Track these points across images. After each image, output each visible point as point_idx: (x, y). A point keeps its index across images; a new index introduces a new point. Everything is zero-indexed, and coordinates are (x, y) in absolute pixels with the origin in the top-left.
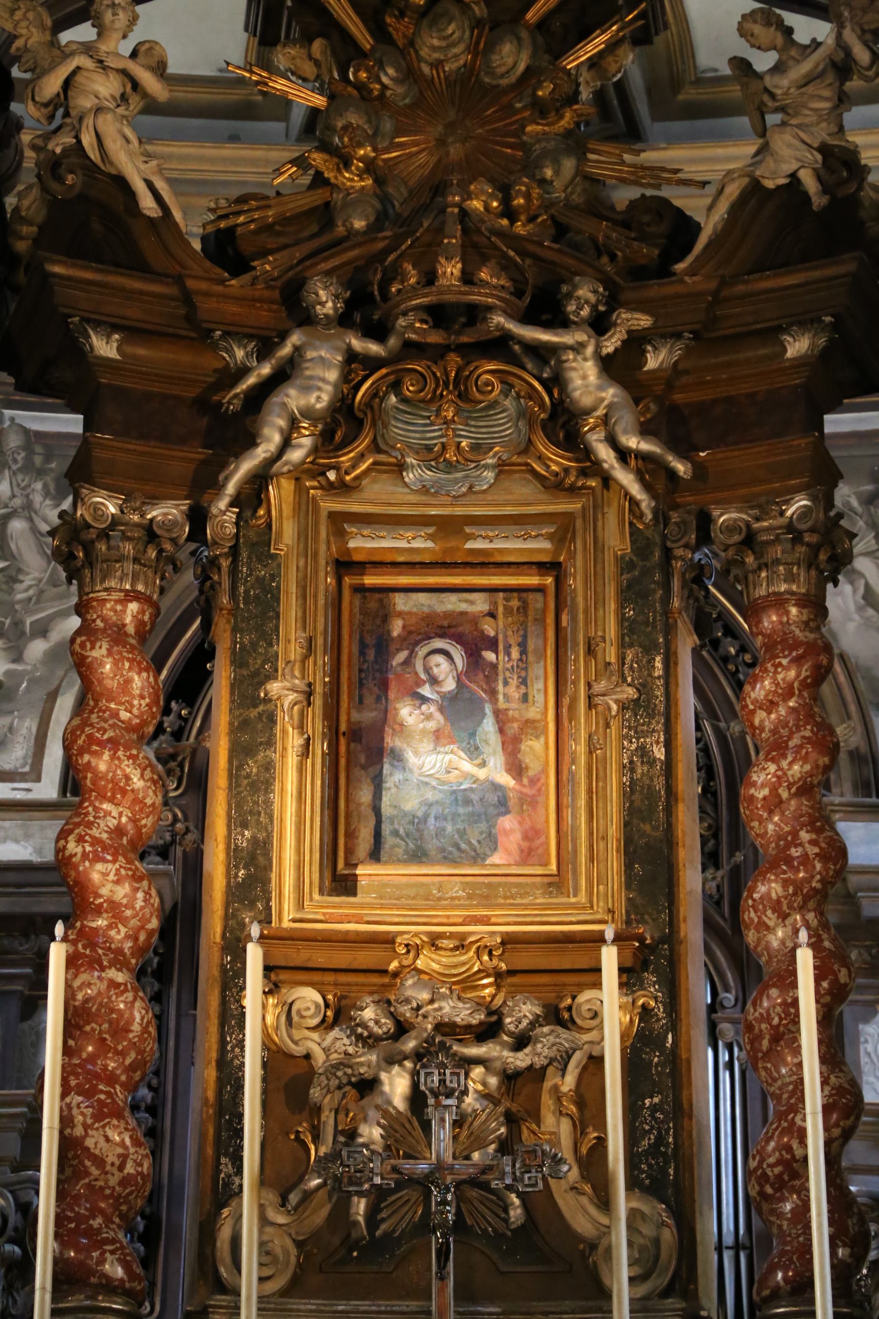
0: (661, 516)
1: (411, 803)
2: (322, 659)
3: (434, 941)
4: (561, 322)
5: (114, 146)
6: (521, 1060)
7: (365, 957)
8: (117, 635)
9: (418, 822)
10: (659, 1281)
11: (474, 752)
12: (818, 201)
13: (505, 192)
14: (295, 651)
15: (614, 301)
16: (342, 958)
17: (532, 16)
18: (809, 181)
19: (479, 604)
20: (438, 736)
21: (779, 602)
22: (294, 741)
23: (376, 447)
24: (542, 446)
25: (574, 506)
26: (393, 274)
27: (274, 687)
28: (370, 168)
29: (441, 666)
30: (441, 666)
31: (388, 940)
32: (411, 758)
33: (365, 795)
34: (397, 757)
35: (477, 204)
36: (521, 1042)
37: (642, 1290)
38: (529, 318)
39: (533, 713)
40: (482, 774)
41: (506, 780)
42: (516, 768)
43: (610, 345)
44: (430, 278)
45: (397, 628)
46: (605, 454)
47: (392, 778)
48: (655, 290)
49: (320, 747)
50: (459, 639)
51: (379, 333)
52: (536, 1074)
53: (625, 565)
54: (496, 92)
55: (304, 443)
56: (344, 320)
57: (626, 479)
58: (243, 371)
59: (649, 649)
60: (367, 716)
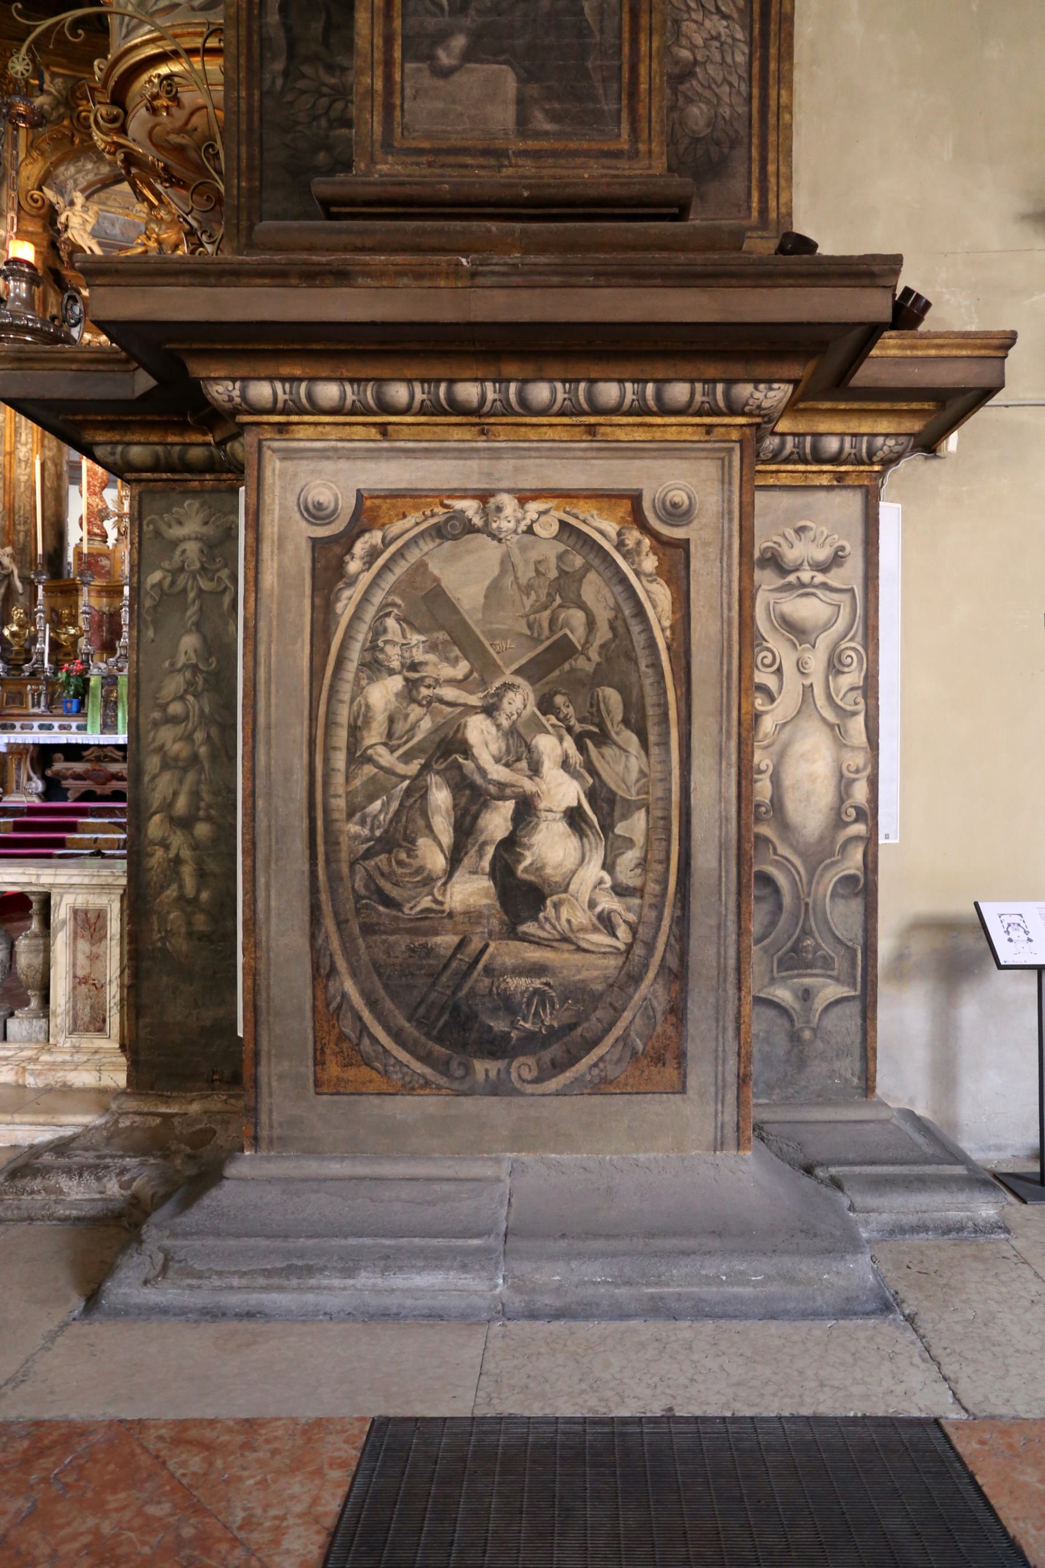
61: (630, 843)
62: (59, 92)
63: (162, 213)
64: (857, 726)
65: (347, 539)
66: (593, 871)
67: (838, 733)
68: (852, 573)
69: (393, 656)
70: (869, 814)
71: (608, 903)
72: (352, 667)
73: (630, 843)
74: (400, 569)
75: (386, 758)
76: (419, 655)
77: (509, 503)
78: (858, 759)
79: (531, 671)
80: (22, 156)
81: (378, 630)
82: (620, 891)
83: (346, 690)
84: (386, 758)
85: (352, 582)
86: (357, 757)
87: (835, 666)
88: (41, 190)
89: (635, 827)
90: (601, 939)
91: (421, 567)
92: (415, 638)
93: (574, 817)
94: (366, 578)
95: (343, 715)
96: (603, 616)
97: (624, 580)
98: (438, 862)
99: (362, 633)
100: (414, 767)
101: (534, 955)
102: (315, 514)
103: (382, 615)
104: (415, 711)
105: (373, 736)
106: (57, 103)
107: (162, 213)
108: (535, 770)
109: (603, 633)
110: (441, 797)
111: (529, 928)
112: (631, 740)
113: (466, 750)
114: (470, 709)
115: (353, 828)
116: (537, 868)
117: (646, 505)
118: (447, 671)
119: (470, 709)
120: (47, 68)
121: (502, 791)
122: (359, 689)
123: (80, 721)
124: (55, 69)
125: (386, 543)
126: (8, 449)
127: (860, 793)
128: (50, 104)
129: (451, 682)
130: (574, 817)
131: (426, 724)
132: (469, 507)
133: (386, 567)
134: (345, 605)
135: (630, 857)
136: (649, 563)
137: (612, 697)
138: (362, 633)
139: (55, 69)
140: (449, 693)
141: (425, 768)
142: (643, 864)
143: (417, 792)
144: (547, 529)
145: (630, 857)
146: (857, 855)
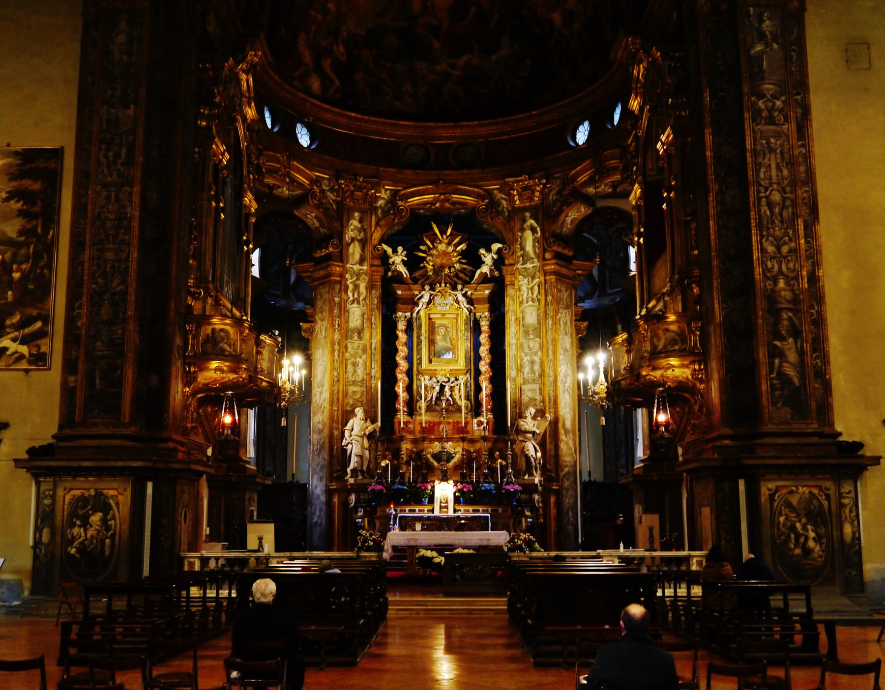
0: (470, 314)
1: (439, 349)
2: (427, 332)
3: (442, 370)
4: (458, 290)
5: (400, 269)
6: (452, 385)
7: (433, 372)
8: (402, 331)
9: (439, 352)
10: (469, 410)
11: (446, 342)
12: (489, 276)
13: (450, 270)
14: (424, 332)
15: (463, 287)
16: (431, 372)
17: (454, 243)
18: (488, 273)
19: (447, 322)
20: (442, 341)
21: (484, 326)
22: (424, 344)
23: (434, 304)
24: (455, 304)
25: (459, 312)
26: (436, 284)
27: (422, 337)
28: (432, 266)
29: (442, 330)
30: (442, 330)
31: (436, 370)
32: (439, 343)
33: (433, 348)
34: (437, 343)
35: (446, 272)
36: (452, 383)
37: (466, 412)
38: (453, 290)
39: (454, 337)
40: (447, 345)
41: (451, 346)
42: (452, 344)
43: (463, 292)
44: (441, 286)
45: (436, 325)
46: (463, 307)
47: (436, 346)
48: (469, 286)
49: (427, 344)
50: (444, 327)
51: (434, 291)
52: (454, 386)
53: (465, 320)
54: (449, 253)
55: (425, 306)
56: (430, 290)
57: (465, 310)
58: (417, 295)
59: (468, 332)
60: (433, 337)
61: (824, 543)
62: (388, 198)
63: (435, 251)
64: (856, 522)
65: (774, 494)
66: (818, 548)
67: (852, 524)
68: (852, 495)
69: (784, 513)
70: (859, 539)
71: (820, 553)
72: (777, 515)
73: (824, 543)
74: (784, 499)
75: (783, 529)
76: (788, 513)
77: (800, 488)
78: (855, 529)
79: (806, 515)
80: (373, 229)
81: (781, 508)
82: (822, 551)
83: (776, 519)
84: (783, 529)
85: (776, 501)
86: (779, 529)
87: (851, 511)
88: (381, 245)
89: (824, 540)
90: (819, 559)
91: (787, 498)
92: (787, 510)
93: (814, 539)
94: (778, 500)
95: (776, 522)
96: (817, 506)
97: (820, 500)
98: (793, 546)
99: (778, 509)
100: (788, 531)
101: (810, 562)
102: (769, 490)
103: (781, 505)
104: (788, 522)
105: (781, 526)
106: (387, 203)
107: (435, 251)
108: (807, 531)
109: (817, 509)
110: (793, 536)
111: (808, 557)
112: (823, 527)
113: (796, 528)
114: (796, 521)
115: (779, 541)
116: (809, 547)
117: (823, 488)
118: (792, 515)
119: (796, 521)
120: (384, 187)
121: (802, 535)
122: (778, 519)
123: (430, 508)
124: (386, 187)
125: (781, 494)
126: (368, 372)
127: (857, 535)
128: (384, 204)
129: (793, 517)
130: (814, 539)
131: (789, 524)
132: (794, 488)
133: (781, 499)
134: (775, 504)
135: (824, 545)
136: (824, 497)
137: (819, 520)
138: (778, 509)
139: (386, 187)
140: (793, 519)
141: (790, 532)
142: (826, 547)
143: (789, 536)
144: (807, 492)
145: (824, 545)
146: (857, 547)
